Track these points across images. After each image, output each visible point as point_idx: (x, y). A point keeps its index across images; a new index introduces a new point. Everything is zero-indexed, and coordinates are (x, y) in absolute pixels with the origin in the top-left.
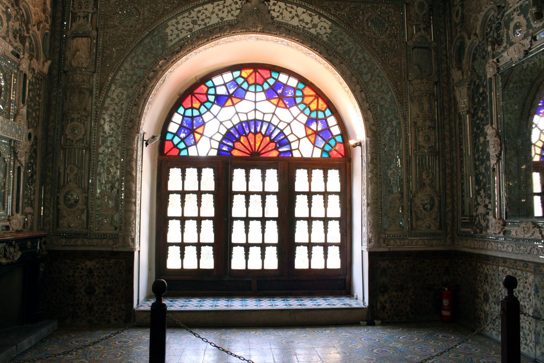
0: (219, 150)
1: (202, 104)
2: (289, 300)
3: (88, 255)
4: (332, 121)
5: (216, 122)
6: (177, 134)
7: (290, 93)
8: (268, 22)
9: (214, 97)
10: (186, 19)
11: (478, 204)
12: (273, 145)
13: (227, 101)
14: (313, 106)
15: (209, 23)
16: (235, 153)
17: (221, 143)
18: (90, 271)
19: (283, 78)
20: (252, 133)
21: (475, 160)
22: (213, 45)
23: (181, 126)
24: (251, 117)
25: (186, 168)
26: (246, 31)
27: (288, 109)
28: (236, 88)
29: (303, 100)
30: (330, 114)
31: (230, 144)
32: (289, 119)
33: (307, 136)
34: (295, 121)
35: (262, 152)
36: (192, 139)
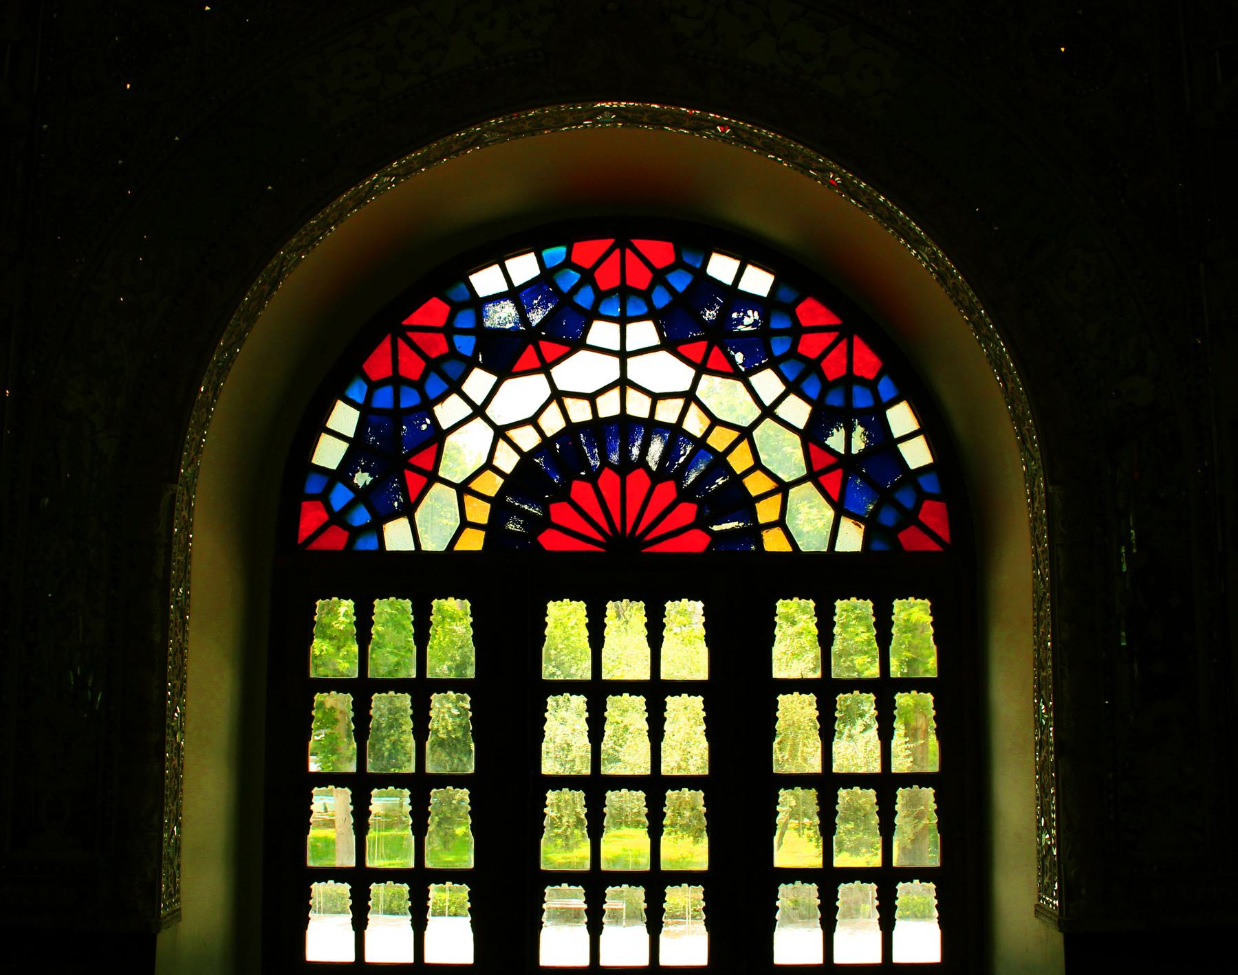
0: (493, 529)
4: (901, 418)
5: (479, 434)
9: (471, 340)
12: (687, 512)
13: (521, 350)
14: (834, 367)
16: (551, 541)
19: (721, 268)
20: (612, 466)
24: (609, 406)
27: (743, 377)
28: (551, 306)
29: (795, 345)
32: (745, 413)
33: (813, 476)
34: (768, 422)
35: (648, 538)
36: (396, 491)
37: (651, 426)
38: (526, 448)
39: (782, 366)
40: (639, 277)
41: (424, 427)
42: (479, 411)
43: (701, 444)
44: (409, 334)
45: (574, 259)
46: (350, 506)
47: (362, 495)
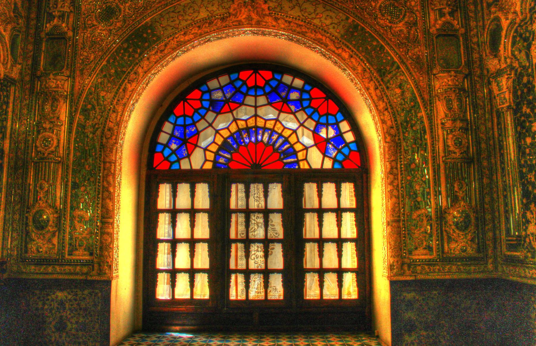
0: (215, 162)
1: (196, 111)
2: (296, 338)
3: (59, 284)
4: (344, 126)
6: (167, 145)
7: (294, 96)
8: (264, 13)
9: (208, 102)
10: (172, 15)
11: (528, 222)
15: (196, 17)
17: (217, 155)
18: (62, 303)
19: (287, 79)
21: (520, 166)
22: (202, 42)
23: (172, 136)
24: (251, 123)
25: (177, 183)
26: (239, 24)
27: (294, 113)
28: (233, 92)
30: (342, 118)
31: (228, 156)
37: (265, 129)
38: (225, 136)
39: (306, 110)
40: (261, 83)
41: (193, 130)
42: (210, 125)
43: (280, 136)
44: (188, 101)
45: (240, 77)
46: (170, 155)
47: (174, 152)
